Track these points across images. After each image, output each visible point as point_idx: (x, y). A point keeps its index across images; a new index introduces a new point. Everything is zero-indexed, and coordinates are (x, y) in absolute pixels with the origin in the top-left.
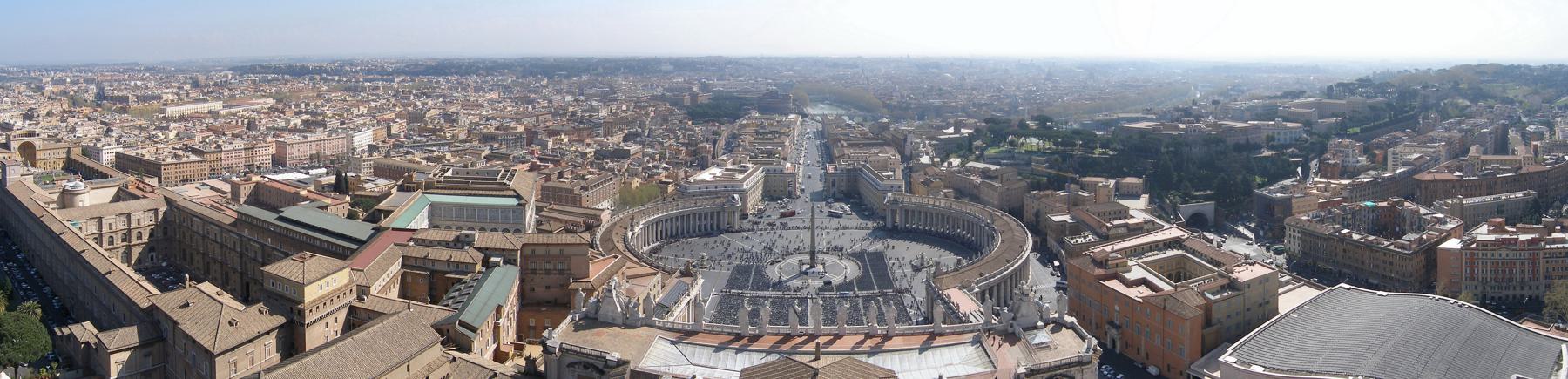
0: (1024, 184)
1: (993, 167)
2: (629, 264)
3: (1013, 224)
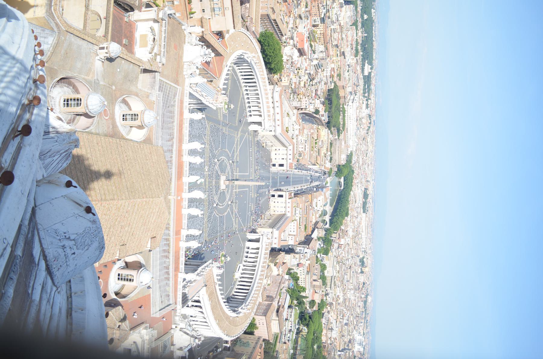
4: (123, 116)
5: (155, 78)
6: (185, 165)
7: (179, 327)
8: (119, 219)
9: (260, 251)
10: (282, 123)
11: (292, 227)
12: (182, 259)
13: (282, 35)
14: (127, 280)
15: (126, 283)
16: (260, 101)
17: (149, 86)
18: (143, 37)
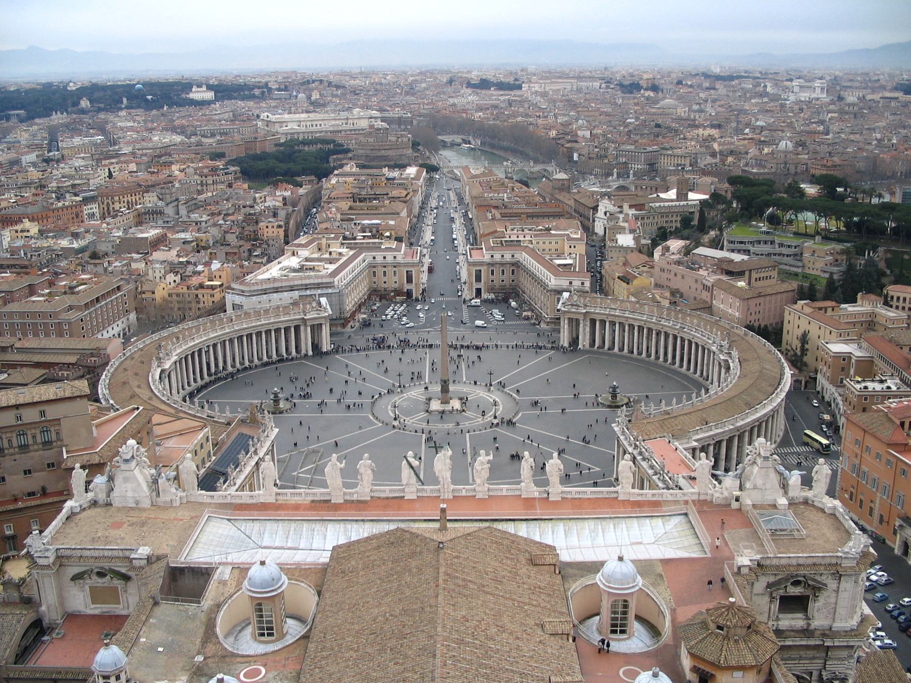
1: (737, 257)
2: (157, 418)
4: (263, 635)
5: (181, 570)
6: (376, 494)
7: (737, 493)
8: (482, 639)
9: (598, 317)
11: (547, 246)
12: (589, 492)
13: (119, 288)
14: (625, 613)
15: (631, 615)
16: (263, 330)
17: (201, 581)
18: (96, 595)
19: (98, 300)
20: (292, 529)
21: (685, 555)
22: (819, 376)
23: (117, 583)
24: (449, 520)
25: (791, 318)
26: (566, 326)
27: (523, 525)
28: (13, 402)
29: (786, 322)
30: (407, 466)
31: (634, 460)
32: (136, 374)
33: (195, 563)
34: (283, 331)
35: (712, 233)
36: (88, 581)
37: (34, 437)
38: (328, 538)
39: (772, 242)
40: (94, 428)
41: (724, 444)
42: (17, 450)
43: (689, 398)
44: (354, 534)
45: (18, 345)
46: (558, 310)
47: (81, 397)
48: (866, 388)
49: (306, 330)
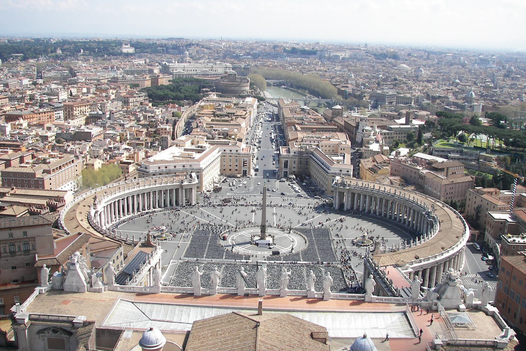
0: (469, 178)
1: (440, 160)
3: (453, 216)
10: (188, 161)
11: (328, 148)
13: (73, 161)
19: (60, 167)
20: (170, 310)
21: (403, 336)
22: (486, 232)
23: (64, 336)
24: (265, 310)
25: (471, 197)
26: (337, 197)
27: (308, 314)
28: (8, 226)
29: (468, 200)
30: (240, 276)
31: (374, 278)
32: (81, 213)
33: (111, 327)
34: (168, 191)
35: (426, 144)
36: (47, 335)
37: (19, 247)
38: (190, 316)
39: (461, 152)
40: (55, 244)
41: (428, 272)
42: (8, 254)
43: (409, 243)
44: (206, 314)
45: (12, 192)
46: (333, 187)
47: (48, 225)
48: (514, 241)
49: (182, 191)
